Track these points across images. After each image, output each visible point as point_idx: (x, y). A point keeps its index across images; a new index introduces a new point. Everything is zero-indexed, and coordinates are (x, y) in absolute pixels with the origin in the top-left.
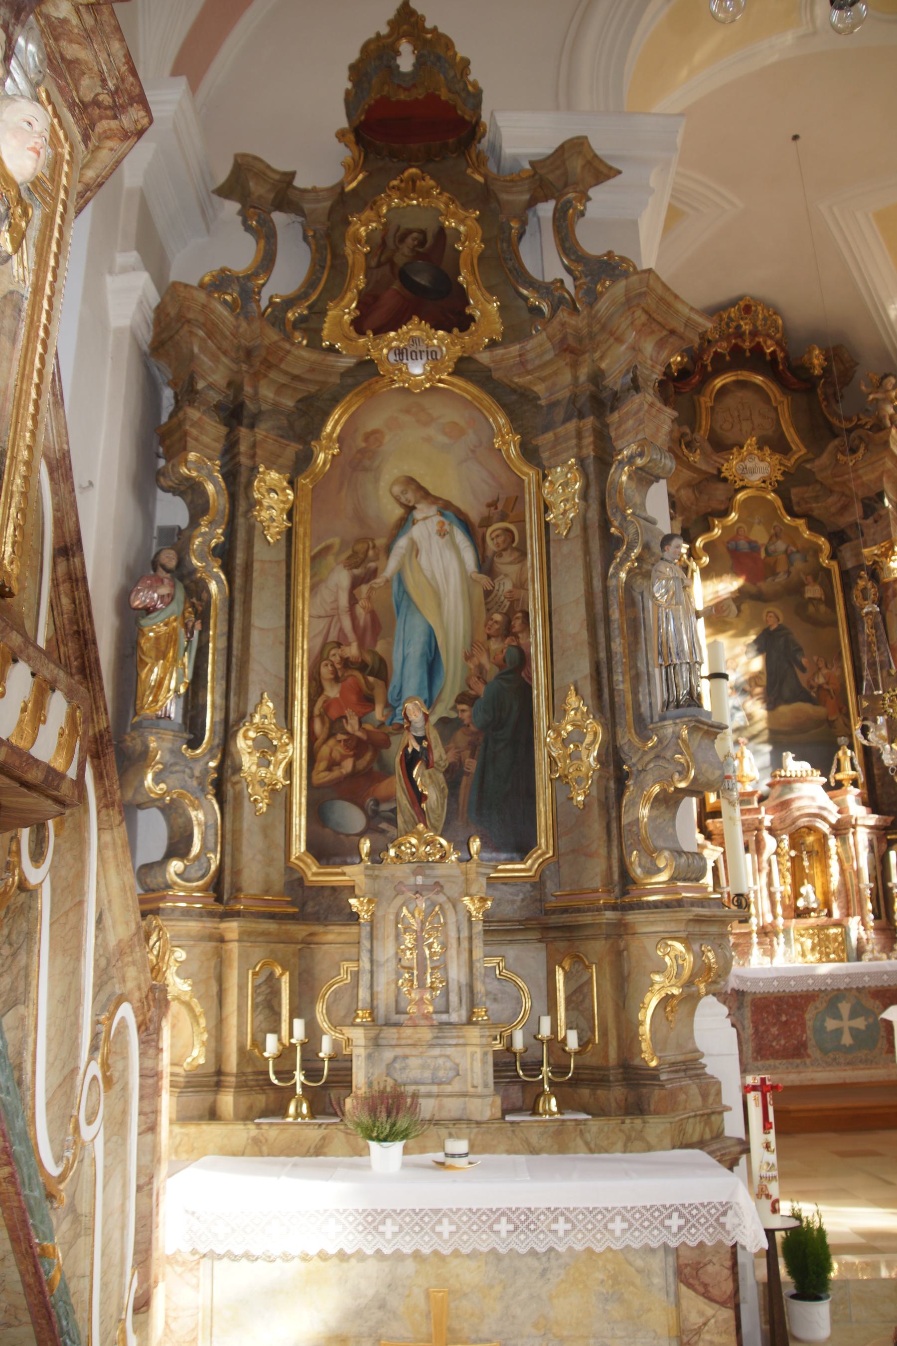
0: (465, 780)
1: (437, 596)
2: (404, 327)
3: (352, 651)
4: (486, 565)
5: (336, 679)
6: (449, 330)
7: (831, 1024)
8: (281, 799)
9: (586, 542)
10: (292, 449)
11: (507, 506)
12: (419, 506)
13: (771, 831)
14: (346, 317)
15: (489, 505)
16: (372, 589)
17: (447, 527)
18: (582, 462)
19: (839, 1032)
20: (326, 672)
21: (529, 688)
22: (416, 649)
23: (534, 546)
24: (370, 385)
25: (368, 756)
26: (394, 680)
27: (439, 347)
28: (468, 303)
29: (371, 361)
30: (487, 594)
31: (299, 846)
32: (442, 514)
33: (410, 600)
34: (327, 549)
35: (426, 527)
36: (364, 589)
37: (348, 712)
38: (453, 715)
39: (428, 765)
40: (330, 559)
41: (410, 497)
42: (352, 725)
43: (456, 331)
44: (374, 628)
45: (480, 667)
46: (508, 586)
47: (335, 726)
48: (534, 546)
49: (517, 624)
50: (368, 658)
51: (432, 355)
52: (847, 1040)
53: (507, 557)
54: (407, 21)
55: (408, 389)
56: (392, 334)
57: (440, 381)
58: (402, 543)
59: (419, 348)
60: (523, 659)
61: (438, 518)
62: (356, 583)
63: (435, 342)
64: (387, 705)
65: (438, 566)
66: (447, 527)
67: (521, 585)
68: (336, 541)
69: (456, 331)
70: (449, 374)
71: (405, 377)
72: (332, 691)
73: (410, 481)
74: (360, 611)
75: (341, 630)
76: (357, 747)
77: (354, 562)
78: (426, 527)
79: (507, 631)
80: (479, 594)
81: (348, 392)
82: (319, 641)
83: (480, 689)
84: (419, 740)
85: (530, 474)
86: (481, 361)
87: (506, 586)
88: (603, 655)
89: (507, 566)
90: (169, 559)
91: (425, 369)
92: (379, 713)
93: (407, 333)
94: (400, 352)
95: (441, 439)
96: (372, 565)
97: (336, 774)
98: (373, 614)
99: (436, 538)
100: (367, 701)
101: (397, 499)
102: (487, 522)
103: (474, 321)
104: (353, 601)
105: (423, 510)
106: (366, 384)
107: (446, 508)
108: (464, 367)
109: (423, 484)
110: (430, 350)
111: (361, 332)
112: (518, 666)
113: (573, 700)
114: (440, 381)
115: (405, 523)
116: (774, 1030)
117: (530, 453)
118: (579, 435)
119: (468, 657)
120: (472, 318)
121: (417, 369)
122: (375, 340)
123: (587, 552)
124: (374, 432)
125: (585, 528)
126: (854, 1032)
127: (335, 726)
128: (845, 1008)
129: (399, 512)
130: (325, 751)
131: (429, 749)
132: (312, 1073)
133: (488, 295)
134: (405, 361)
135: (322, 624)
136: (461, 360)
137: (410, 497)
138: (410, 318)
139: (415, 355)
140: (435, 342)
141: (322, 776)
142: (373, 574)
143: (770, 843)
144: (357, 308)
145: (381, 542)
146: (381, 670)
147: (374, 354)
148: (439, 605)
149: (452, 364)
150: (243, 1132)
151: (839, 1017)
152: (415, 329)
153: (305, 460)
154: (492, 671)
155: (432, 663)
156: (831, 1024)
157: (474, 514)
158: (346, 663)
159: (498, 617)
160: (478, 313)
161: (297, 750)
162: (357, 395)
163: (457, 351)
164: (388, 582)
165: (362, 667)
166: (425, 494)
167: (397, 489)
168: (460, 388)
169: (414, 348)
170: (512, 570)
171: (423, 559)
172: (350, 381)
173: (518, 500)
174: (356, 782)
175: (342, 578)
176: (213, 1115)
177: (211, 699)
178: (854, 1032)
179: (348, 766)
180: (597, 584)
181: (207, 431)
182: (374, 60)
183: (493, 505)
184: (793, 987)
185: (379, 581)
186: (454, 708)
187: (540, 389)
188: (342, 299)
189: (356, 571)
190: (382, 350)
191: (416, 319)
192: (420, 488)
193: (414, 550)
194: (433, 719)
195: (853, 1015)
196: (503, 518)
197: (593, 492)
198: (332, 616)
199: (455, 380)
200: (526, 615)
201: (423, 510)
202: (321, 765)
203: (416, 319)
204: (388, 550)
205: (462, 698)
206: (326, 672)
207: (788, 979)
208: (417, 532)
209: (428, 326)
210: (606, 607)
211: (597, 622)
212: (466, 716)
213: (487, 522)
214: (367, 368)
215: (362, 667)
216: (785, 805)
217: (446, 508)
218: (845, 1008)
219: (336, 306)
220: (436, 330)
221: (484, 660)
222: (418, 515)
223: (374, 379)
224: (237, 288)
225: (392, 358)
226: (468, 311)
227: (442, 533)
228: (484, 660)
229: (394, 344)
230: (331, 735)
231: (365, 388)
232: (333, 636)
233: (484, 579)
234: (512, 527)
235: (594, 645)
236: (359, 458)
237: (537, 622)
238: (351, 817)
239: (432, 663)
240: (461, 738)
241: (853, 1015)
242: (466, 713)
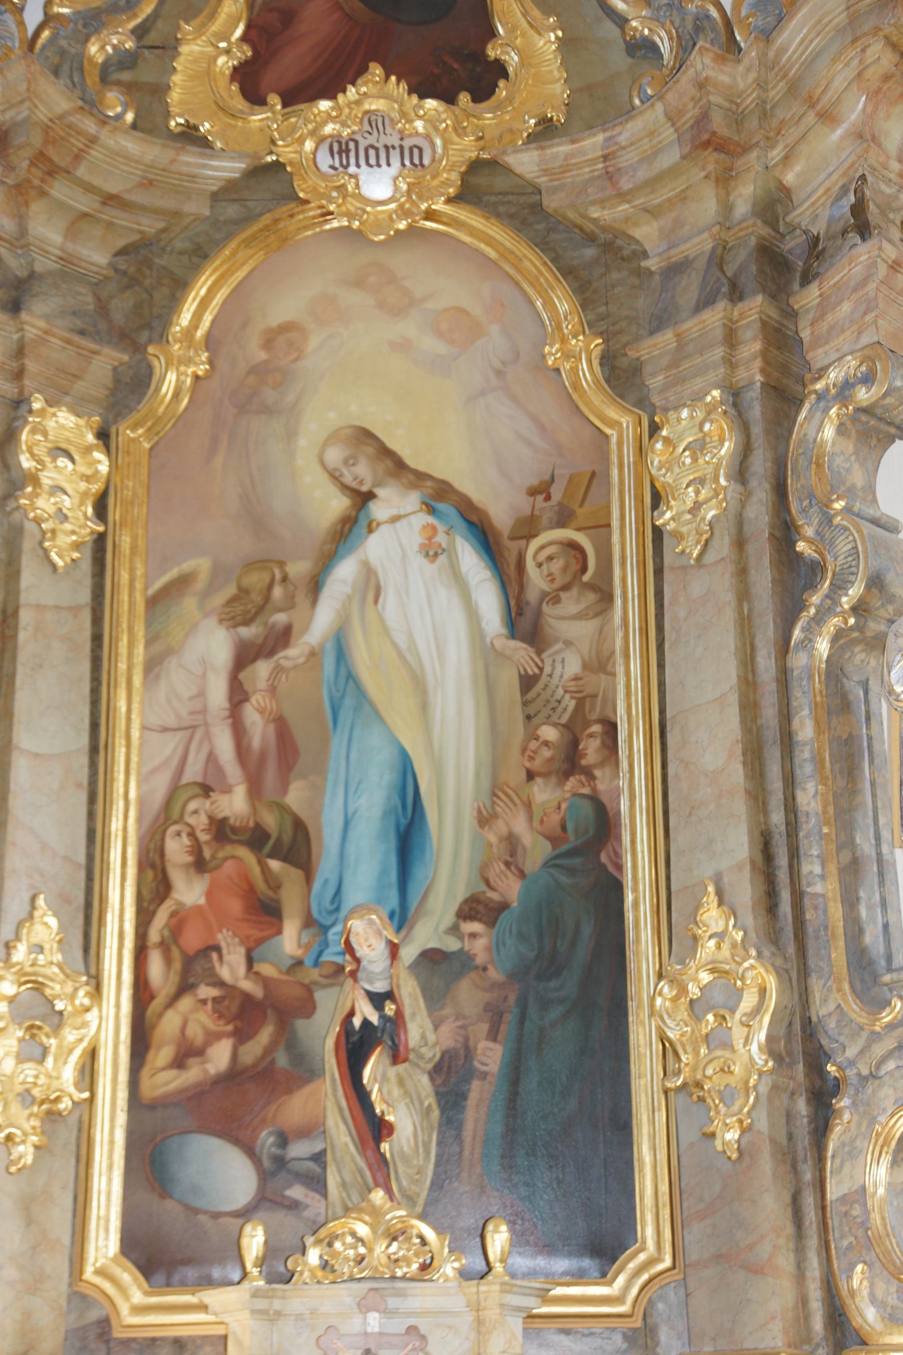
0: (476, 1091)
1: (419, 685)
2: (351, 91)
3: (235, 804)
4: (524, 621)
5: (200, 865)
6: (449, 99)
8: (67, 1134)
9: (742, 572)
12: (380, 492)
14: (222, 60)
15: (533, 492)
16: (279, 669)
17: (441, 538)
18: (735, 396)
20: (176, 849)
21: (618, 887)
22: (372, 802)
23: (627, 580)
24: (276, 221)
25: (265, 1035)
26: (326, 868)
27: (427, 137)
28: (492, 34)
29: (278, 166)
30: (528, 682)
31: (105, 1243)
32: (431, 510)
33: (361, 693)
34: (182, 583)
35: (398, 532)
36: (262, 669)
37: (224, 938)
38: (452, 945)
39: (396, 1058)
40: (190, 603)
41: (363, 472)
42: (232, 967)
43: (464, 98)
44: (283, 754)
45: (511, 842)
46: (572, 666)
47: (194, 968)
48: (627, 580)
49: (591, 749)
50: (270, 820)
51: (413, 155)
53: (571, 603)
55: (359, 232)
56: (324, 105)
57: (430, 215)
58: (345, 571)
59: (384, 140)
60: (604, 825)
61: (425, 519)
62: (245, 657)
63: (419, 125)
64: (309, 922)
65: (421, 620)
66: (441, 538)
67: (600, 664)
68: (202, 565)
69: (464, 98)
70: (449, 201)
71: (352, 205)
72: (189, 892)
74: (252, 716)
75: (211, 758)
76: (243, 1014)
77: (242, 609)
78: (398, 532)
79: (570, 763)
80: (509, 681)
81: (229, 237)
82: (161, 784)
83: (511, 889)
84: (377, 1000)
85: (620, 422)
86: (519, 170)
87: (566, 666)
88: (777, 818)
89: (570, 623)
91: (396, 188)
92: (290, 939)
93: (358, 103)
94: (342, 148)
95: (431, 344)
96: (280, 618)
97: (193, 1074)
98: (282, 727)
99: (418, 561)
100: (266, 912)
101: (335, 477)
102: (527, 528)
103: (505, 75)
104: (238, 695)
105: (391, 501)
106: (267, 219)
107: (440, 495)
108: (481, 184)
109: (391, 444)
110: (407, 143)
111: (255, 97)
113: (712, 916)
114: (430, 215)
115: (350, 528)
118: (731, 338)
119: (484, 820)
120: (500, 70)
121: (379, 185)
122: (286, 117)
123: (744, 594)
124: (286, 328)
125: (740, 543)
127: (194, 968)
129: (338, 504)
130: (169, 1025)
131: (397, 1022)
133: (536, 13)
134: (352, 169)
135: (170, 745)
136: (475, 166)
137: (363, 472)
138: (363, 70)
139: (376, 156)
140: (419, 125)
141: (162, 1080)
142: (283, 637)
144: (244, 38)
145: (298, 569)
146: (296, 846)
147: (285, 152)
148: (424, 706)
149: (455, 177)
152: (375, 94)
153: (134, 385)
154: (536, 851)
155: (408, 835)
157: (502, 508)
158: (222, 830)
159: (549, 733)
160: (512, 59)
161: (109, 1022)
162: (247, 243)
163: (466, 148)
164: (314, 654)
165: (257, 838)
166: (396, 467)
167: (334, 455)
168: (472, 231)
169: (372, 140)
170: (582, 631)
171: (390, 605)
172: (232, 211)
173: (594, 480)
175: (215, 645)
179: (220, 1056)
180: (766, 664)
183: (541, 490)
185: (294, 653)
186: (454, 930)
187: (647, 233)
188: (212, 16)
189: (246, 632)
190: (301, 141)
191: (376, 70)
192: (385, 452)
193: (371, 586)
194: (409, 954)
196: (564, 519)
197: (760, 463)
198: (193, 728)
199: (462, 213)
200: (611, 728)
201: (391, 501)
202: (161, 1055)
203: (376, 70)
204: (315, 586)
205: (474, 909)
206: (176, 849)
208: (377, 548)
209: (403, 86)
210: (786, 715)
211: (766, 747)
212: (479, 948)
213: (527, 528)
214: (269, 182)
215: (257, 838)
217: (440, 495)
219: (200, 31)
220: (422, 97)
221: (520, 826)
222: (378, 510)
223: (285, 209)
225: (324, 161)
226: (492, 52)
227: (431, 552)
228: (520, 826)
229: (329, 129)
230: (184, 988)
231: (266, 228)
232: (193, 772)
233: (521, 651)
234: (581, 539)
235: (758, 797)
236: (254, 385)
237: (634, 742)
238: (223, 1172)
239: (408, 835)
240: (469, 996)
242: (479, 940)
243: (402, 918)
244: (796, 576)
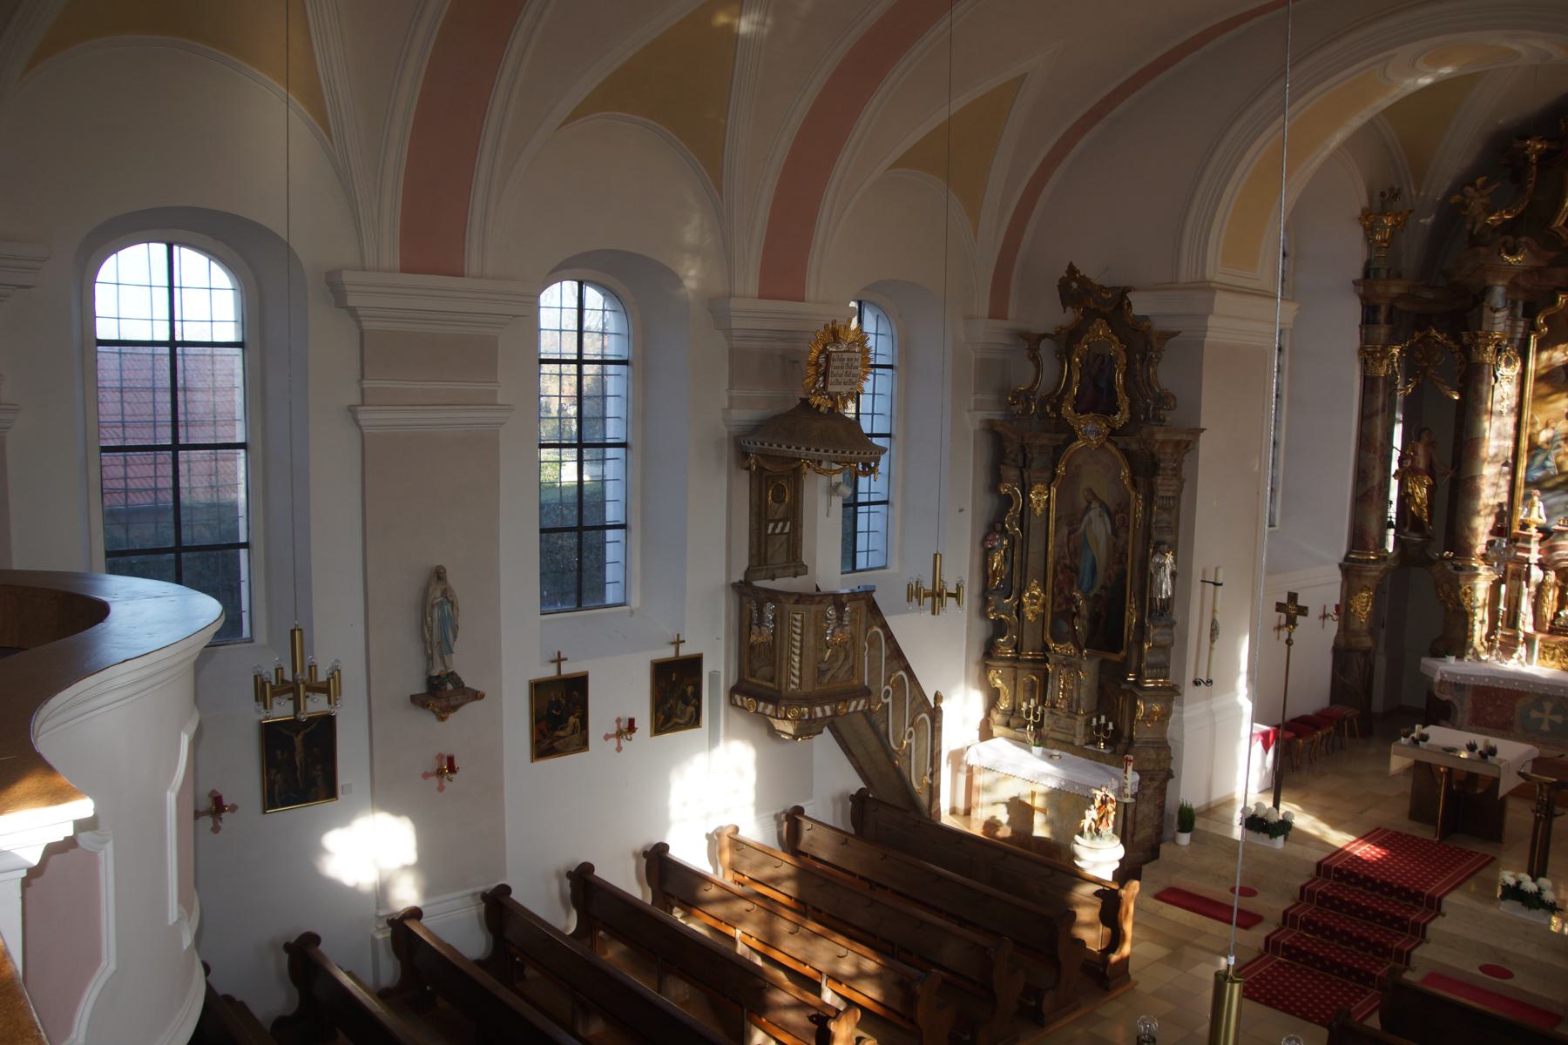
4: (1115, 532)
7: (1534, 714)
10: (1047, 475)
11: (1124, 507)
13: (1542, 565)
19: (1541, 721)
35: (1094, 512)
47: (1061, 591)
52: (1545, 727)
54: (1072, 270)
65: (1098, 528)
72: (1061, 577)
73: (1090, 490)
78: (1094, 512)
85: (1133, 494)
90: (999, 527)
100: (1072, 582)
105: (1094, 504)
107: (1102, 504)
112: (1122, 576)
115: (1088, 509)
116: (1490, 709)
117: (1134, 483)
126: (1552, 724)
127: (1061, 591)
128: (1548, 706)
129: (1083, 503)
132: (1036, 717)
143: (1536, 574)
146: (1075, 570)
150: (1011, 732)
151: (1543, 711)
153: (1054, 475)
156: (1534, 714)
157: (1112, 509)
166: (1095, 497)
173: (1128, 504)
174: (1060, 616)
175: (1065, 530)
176: (1008, 725)
177: (1016, 578)
178: (1552, 724)
181: (1013, 473)
182: (1064, 286)
184: (1501, 684)
193: (1090, 522)
195: (1554, 712)
201: (1094, 504)
207: (1498, 679)
216: (1552, 549)
217: (1102, 504)
218: (1548, 706)
224: (1026, 396)
241: (1554, 712)
243: (1091, 588)
244: (1150, 537)
